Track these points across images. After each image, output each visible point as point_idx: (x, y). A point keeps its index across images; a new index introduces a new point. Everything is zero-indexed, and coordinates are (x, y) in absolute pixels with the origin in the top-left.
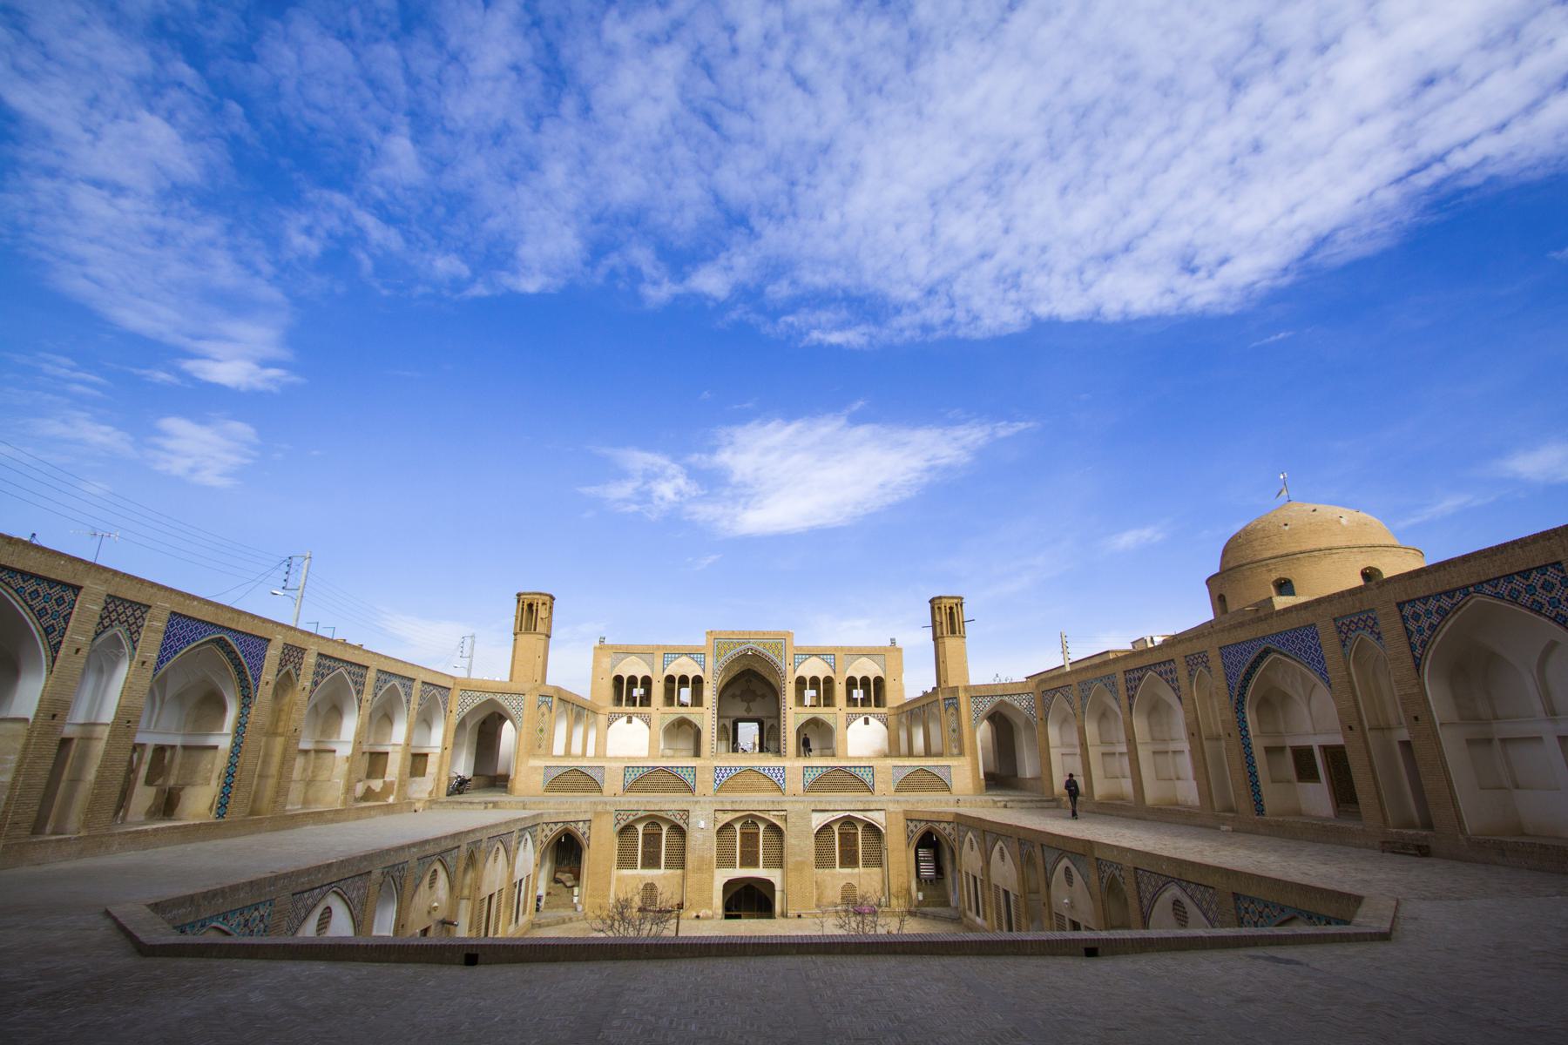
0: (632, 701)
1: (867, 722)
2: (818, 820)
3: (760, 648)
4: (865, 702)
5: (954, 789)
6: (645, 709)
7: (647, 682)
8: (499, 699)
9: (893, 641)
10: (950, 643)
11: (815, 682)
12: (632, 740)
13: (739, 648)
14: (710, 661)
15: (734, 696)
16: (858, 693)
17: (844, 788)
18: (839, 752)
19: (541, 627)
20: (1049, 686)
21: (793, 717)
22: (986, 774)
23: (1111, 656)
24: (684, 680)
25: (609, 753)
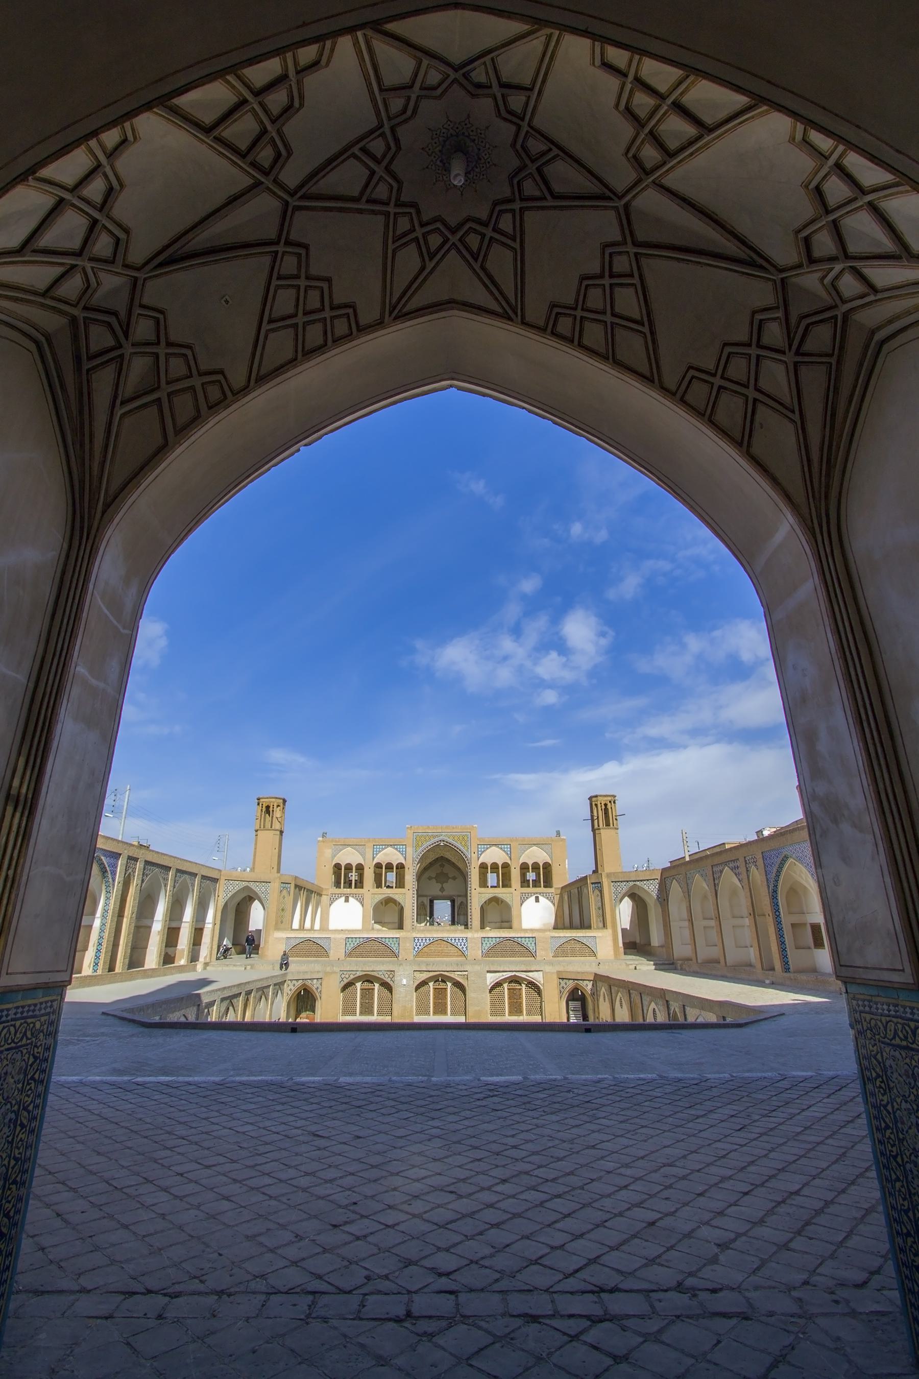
0: (349, 884)
1: (537, 900)
2: (491, 979)
3: (450, 840)
4: (536, 883)
5: (598, 956)
6: (359, 891)
7: (360, 868)
8: (251, 885)
9: (558, 833)
10: (605, 833)
11: (495, 867)
12: (347, 915)
13: (433, 841)
14: (410, 850)
15: (430, 878)
16: (531, 876)
17: (513, 954)
18: (515, 924)
19: (277, 826)
20: (676, 871)
21: (477, 896)
22: (624, 943)
23: (727, 847)
24: (389, 867)
25: (331, 927)
